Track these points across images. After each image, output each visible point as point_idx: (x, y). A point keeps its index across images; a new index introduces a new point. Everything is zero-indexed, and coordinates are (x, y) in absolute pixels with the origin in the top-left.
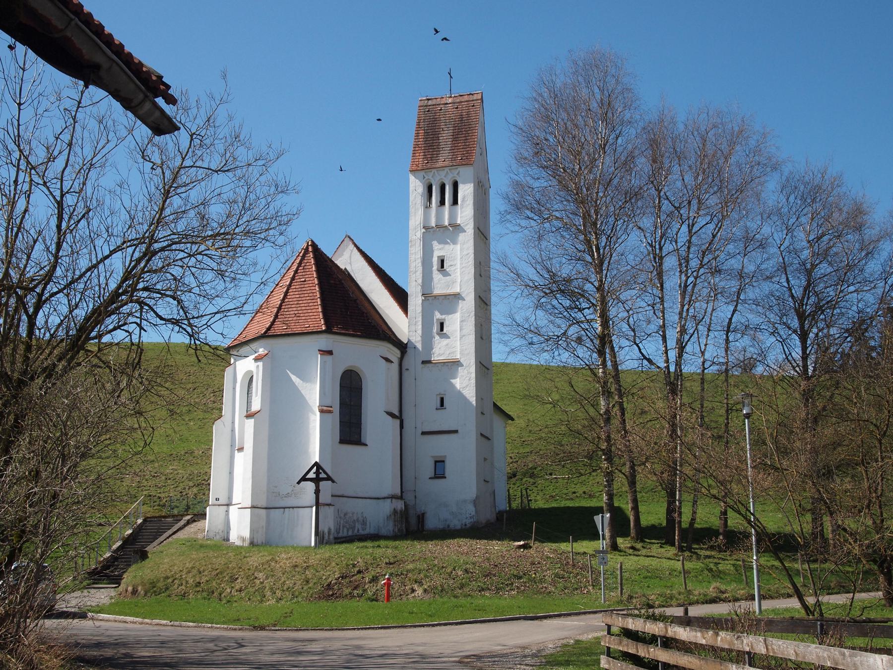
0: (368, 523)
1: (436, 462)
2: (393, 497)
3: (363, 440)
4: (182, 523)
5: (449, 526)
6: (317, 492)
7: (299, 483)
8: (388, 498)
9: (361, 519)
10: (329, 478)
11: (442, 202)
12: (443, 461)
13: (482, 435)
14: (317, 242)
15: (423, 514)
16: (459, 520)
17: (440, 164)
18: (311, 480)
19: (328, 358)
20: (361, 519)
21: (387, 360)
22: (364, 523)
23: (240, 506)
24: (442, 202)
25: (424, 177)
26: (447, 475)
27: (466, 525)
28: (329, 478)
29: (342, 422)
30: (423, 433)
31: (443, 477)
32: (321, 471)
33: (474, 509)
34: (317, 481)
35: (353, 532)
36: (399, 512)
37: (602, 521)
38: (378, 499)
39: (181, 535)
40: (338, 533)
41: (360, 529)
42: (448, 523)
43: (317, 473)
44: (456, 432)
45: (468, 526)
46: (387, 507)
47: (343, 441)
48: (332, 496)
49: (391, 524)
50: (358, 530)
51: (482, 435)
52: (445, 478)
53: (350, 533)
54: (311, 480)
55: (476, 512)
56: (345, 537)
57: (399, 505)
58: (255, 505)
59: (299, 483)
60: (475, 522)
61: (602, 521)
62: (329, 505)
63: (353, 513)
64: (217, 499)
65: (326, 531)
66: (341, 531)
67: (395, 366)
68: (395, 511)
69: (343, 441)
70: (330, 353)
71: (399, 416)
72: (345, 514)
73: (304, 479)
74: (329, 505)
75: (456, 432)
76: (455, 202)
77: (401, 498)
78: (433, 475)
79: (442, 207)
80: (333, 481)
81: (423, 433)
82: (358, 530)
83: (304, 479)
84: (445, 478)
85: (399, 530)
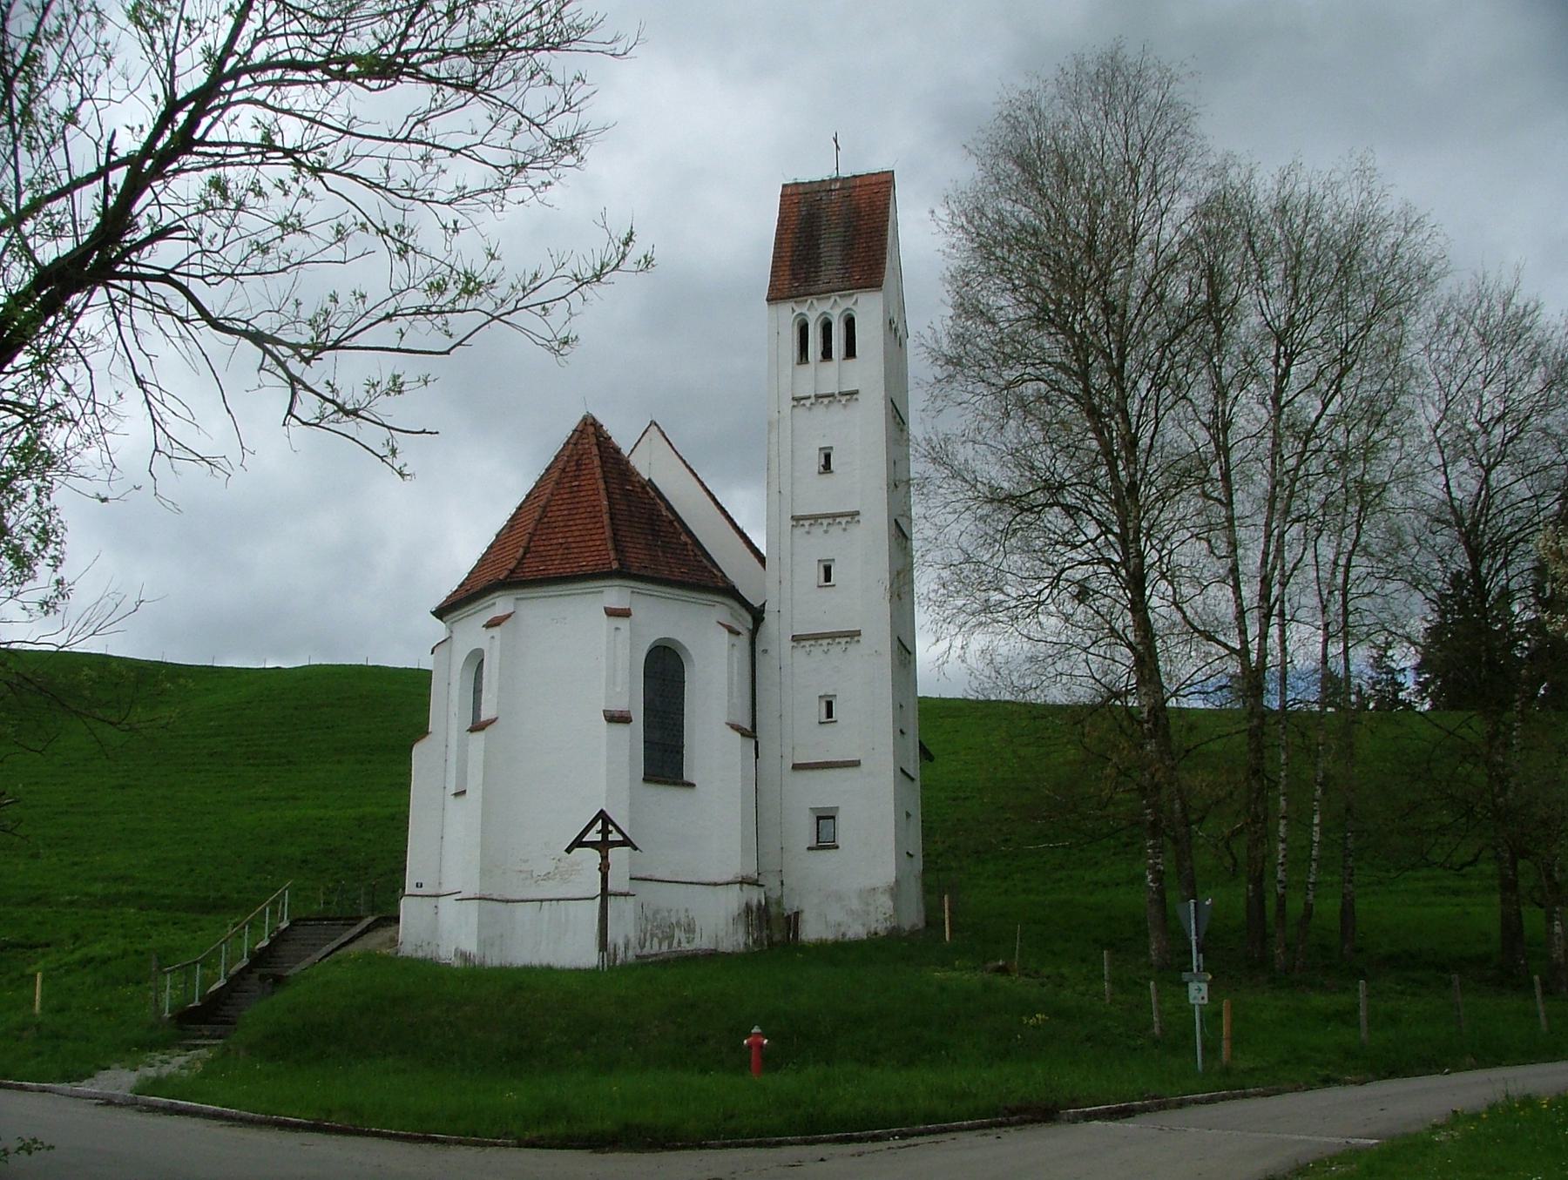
0: (698, 930)
1: (819, 818)
2: (743, 882)
3: (686, 778)
4: (357, 929)
5: (844, 935)
6: (604, 868)
7: (569, 850)
8: (735, 883)
9: (683, 920)
10: (626, 842)
11: (827, 354)
12: (833, 818)
13: (902, 770)
14: (600, 420)
15: (797, 914)
16: (864, 925)
17: (823, 287)
18: (592, 844)
19: (623, 623)
20: (683, 920)
21: (732, 631)
22: (690, 929)
23: (458, 896)
24: (827, 354)
25: (793, 311)
26: (839, 842)
27: (876, 934)
28: (626, 842)
29: (649, 743)
30: (796, 767)
31: (859, 761)
32: (610, 827)
33: (890, 904)
34: (603, 846)
35: (670, 946)
36: (754, 909)
37: (733, 1176)
38: (715, 884)
39: (355, 948)
40: (642, 947)
41: (683, 940)
42: (843, 930)
43: (605, 832)
44: (856, 764)
45: (882, 933)
46: (733, 900)
47: (648, 779)
48: (631, 879)
49: (741, 929)
50: (679, 942)
51: (902, 770)
52: (837, 847)
53: (665, 948)
54: (592, 844)
55: (895, 909)
56: (656, 955)
57: (755, 896)
58: (486, 893)
59: (569, 850)
60: (894, 928)
61: (733, 1176)
62: (626, 895)
63: (669, 911)
64: (419, 885)
65: (621, 943)
66: (648, 944)
67: (744, 640)
68: (748, 907)
69: (648, 779)
70: (624, 614)
71: (750, 733)
72: (656, 912)
73: (579, 843)
74: (626, 895)
75: (856, 764)
76: (850, 352)
77: (755, 883)
78: (814, 843)
79: (827, 364)
80: (636, 848)
81: (796, 767)
82: (679, 942)
83: (579, 843)
84: (837, 847)
85: (754, 942)
